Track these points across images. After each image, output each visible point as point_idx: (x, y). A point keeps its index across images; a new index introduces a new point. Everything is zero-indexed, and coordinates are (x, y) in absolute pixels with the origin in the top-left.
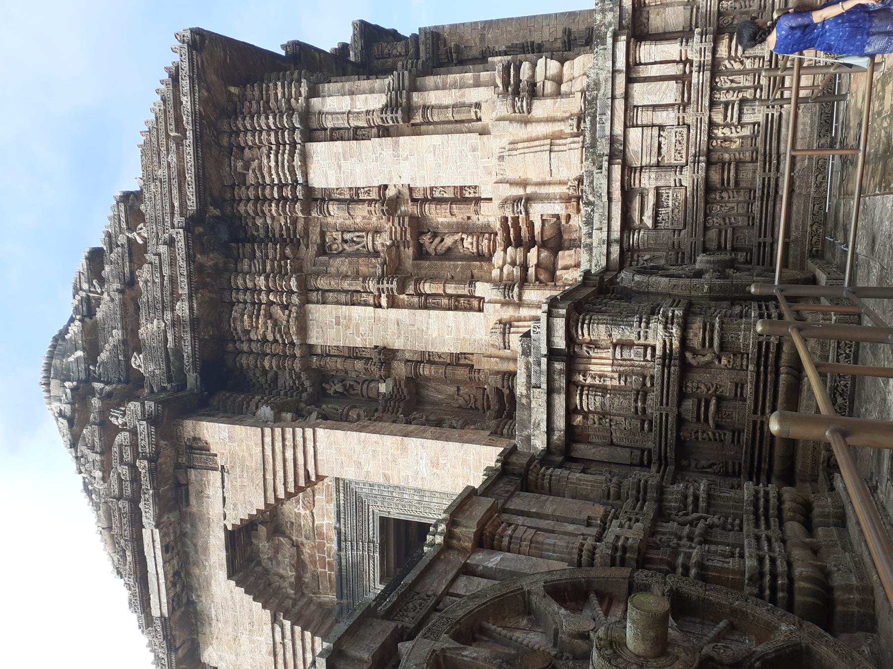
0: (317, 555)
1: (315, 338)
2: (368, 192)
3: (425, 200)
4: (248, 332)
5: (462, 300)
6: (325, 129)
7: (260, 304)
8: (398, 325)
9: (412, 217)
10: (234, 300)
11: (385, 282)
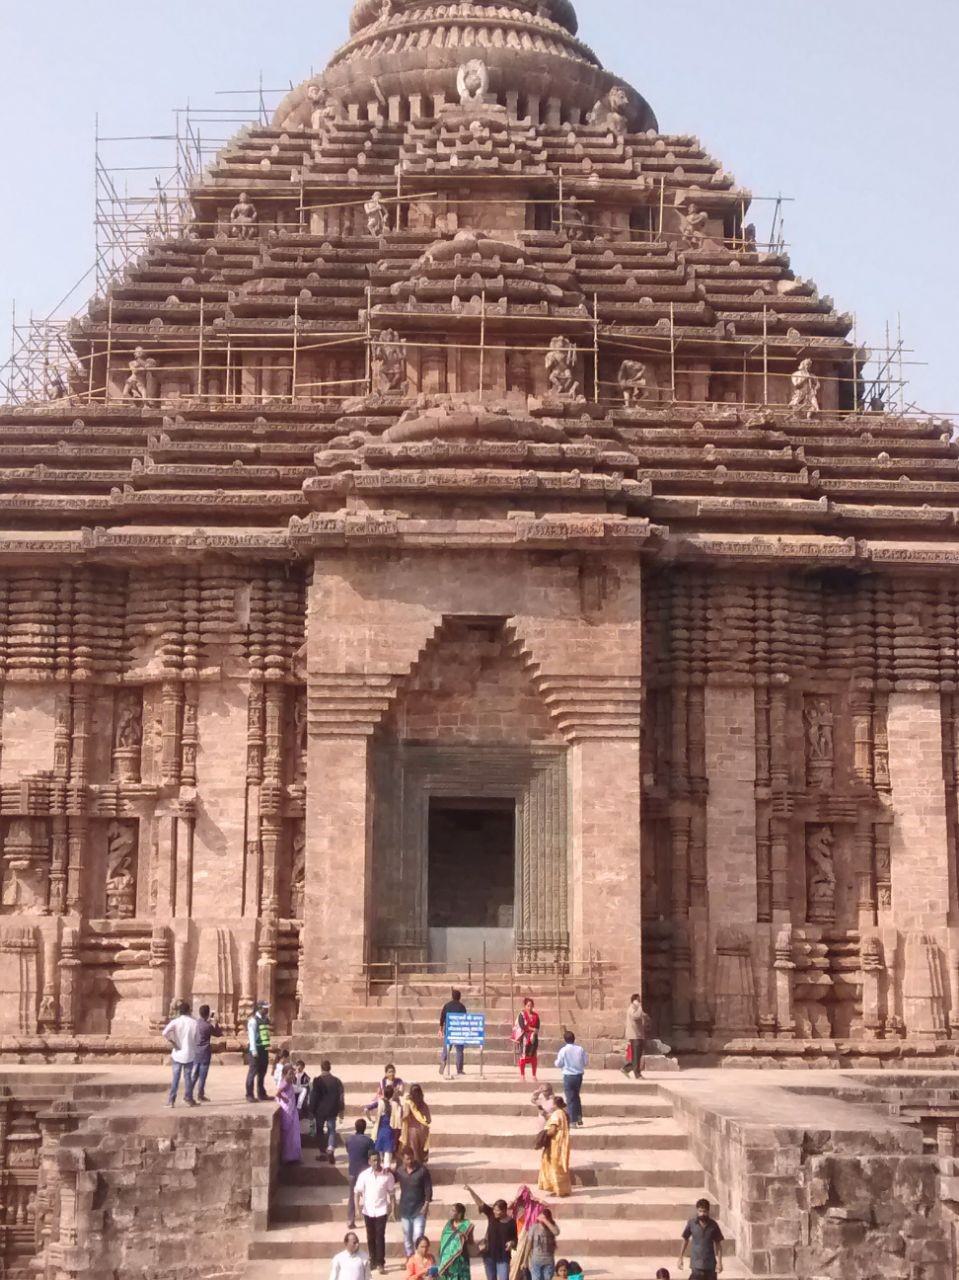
0: (459, 714)
1: (713, 699)
2: (883, 769)
3: (874, 840)
4: (719, 608)
5: (766, 891)
6: (953, 713)
7: (754, 630)
8: (738, 812)
9: (853, 826)
10: (757, 592)
11: (791, 802)
